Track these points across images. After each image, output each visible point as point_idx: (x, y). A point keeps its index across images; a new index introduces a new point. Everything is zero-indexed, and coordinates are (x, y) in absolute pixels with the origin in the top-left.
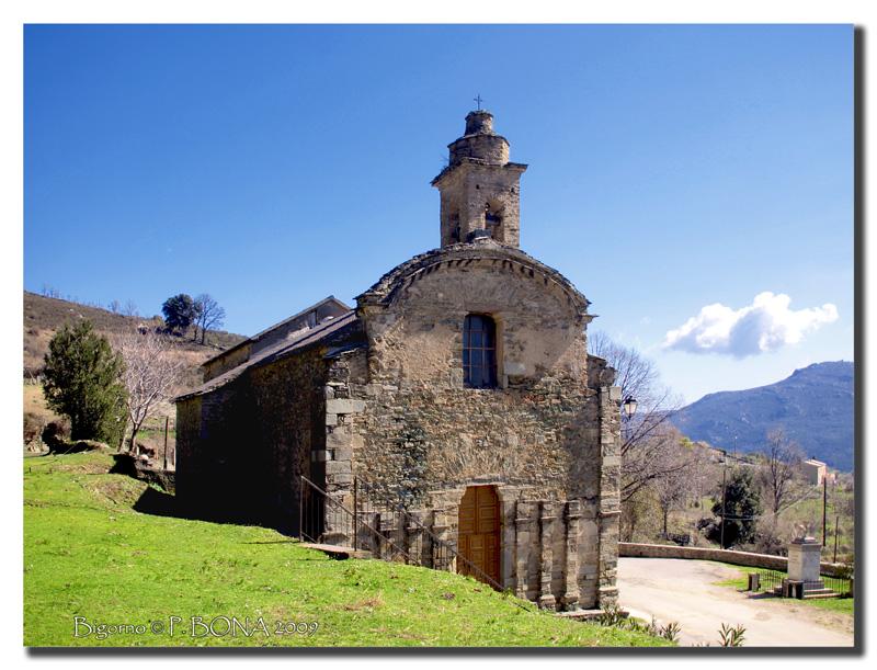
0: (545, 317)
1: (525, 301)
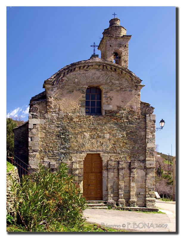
0: (121, 87)
1: (113, 81)
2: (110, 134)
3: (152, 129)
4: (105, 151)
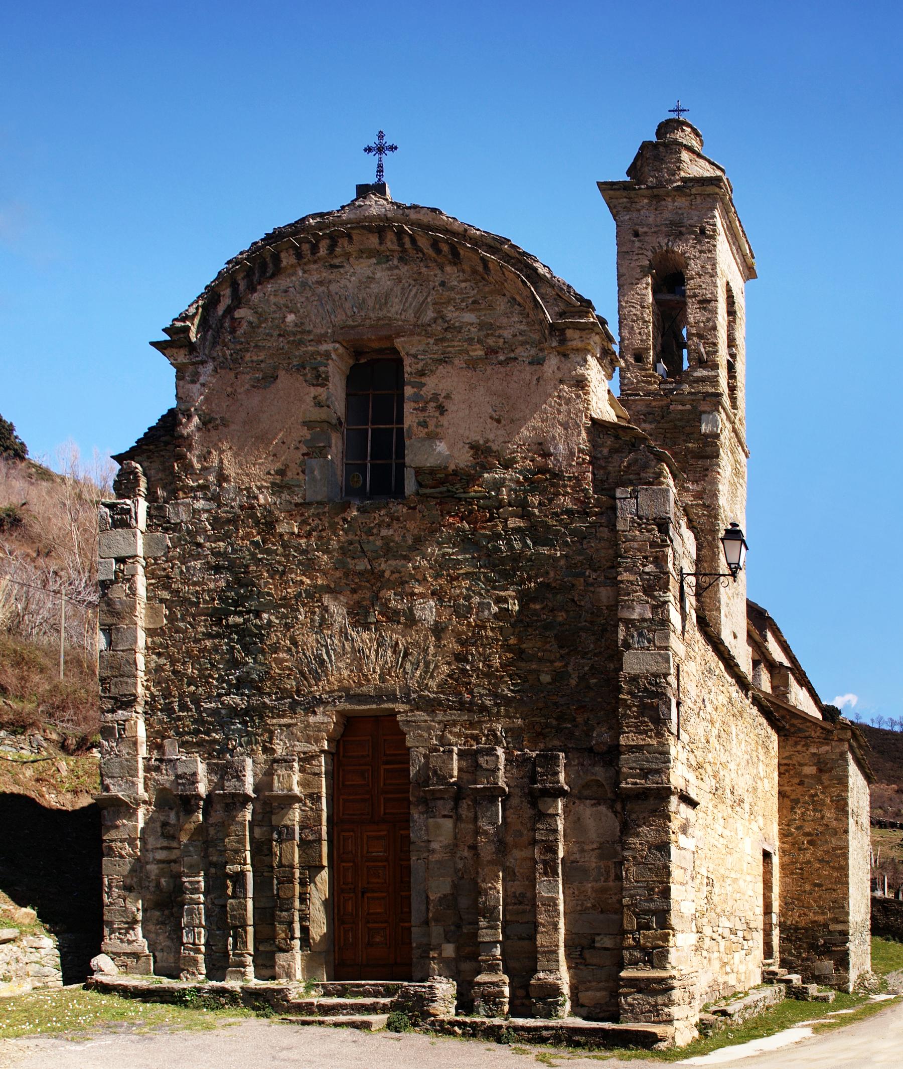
0: (491, 341)
1: (450, 313)
2: (441, 600)
3: (650, 568)
4: (420, 696)
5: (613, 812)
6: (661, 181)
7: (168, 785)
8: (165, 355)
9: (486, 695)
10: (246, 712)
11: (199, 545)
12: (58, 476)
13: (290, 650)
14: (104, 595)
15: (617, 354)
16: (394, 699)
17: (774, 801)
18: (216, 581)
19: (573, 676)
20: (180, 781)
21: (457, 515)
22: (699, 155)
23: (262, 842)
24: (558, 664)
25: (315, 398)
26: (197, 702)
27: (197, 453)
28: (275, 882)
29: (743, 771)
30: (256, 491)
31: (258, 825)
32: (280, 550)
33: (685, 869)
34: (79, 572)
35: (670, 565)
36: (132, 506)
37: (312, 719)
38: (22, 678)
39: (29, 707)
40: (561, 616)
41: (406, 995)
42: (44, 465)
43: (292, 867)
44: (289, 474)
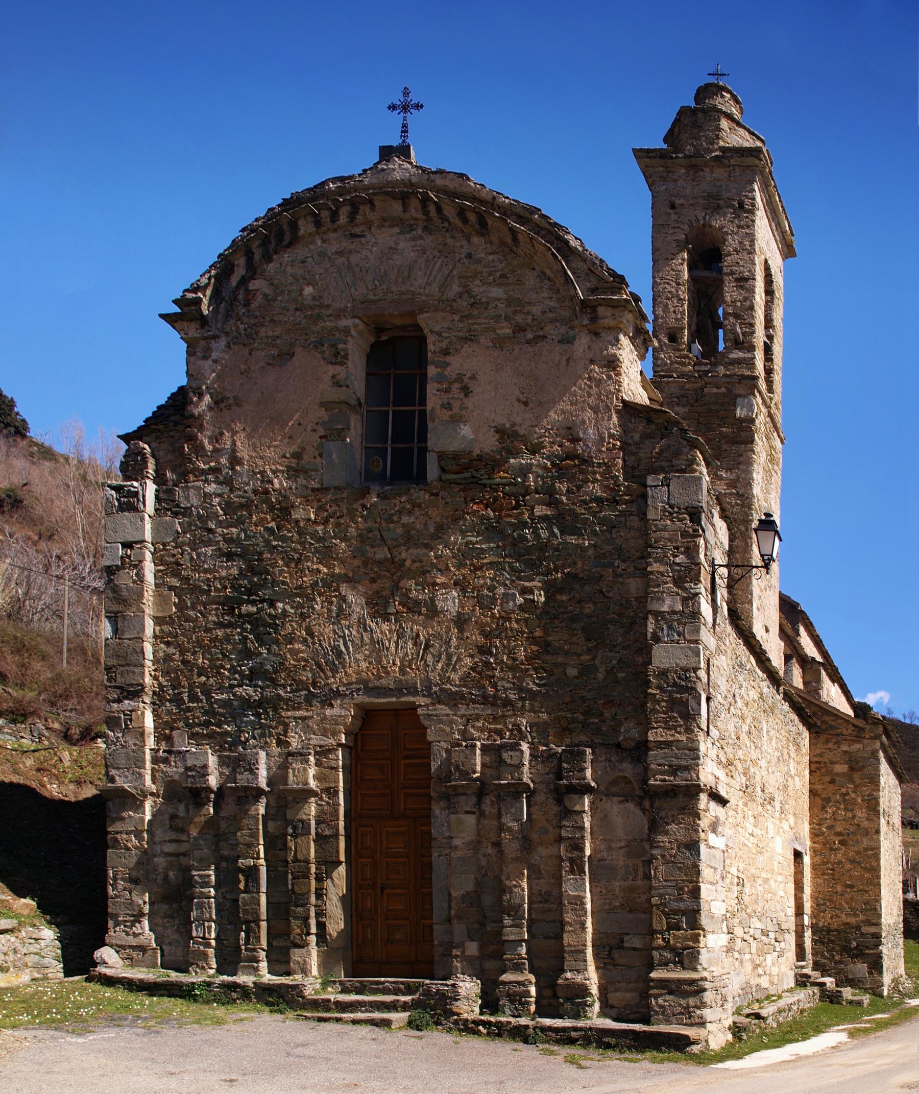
0: (519, 318)
1: (477, 288)
2: (464, 590)
3: (681, 559)
4: (441, 690)
5: (641, 809)
6: (698, 150)
7: (177, 777)
8: (175, 328)
9: (511, 689)
10: (260, 703)
11: (210, 531)
12: (62, 455)
13: (305, 640)
14: (110, 581)
15: (651, 333)
16: (414, 691)
17: (806, 798)
18: (228, 568)
19: (600, 670)
20: (190, 773)
21: (481, 502)
22: (738, 124)
23: (276, 837)
24: (585, 658)
25: (333, 377)
26: (207, 693)
27: (208, 433)
28: (290, 877)
29: (774, 768)
30: (271, 475)
31: (272, 819)
32: (296, 536)
33: (715, 869)
34: (84, 557)
35: (702, 556)
36: (140, 488)
37: (328, 712)
38: (23, 665)
39: (30, 695)
40: (589, 608)
41: (427, 993)
42: (47, 444)
43: (308, 862)
44: (305, 457)
